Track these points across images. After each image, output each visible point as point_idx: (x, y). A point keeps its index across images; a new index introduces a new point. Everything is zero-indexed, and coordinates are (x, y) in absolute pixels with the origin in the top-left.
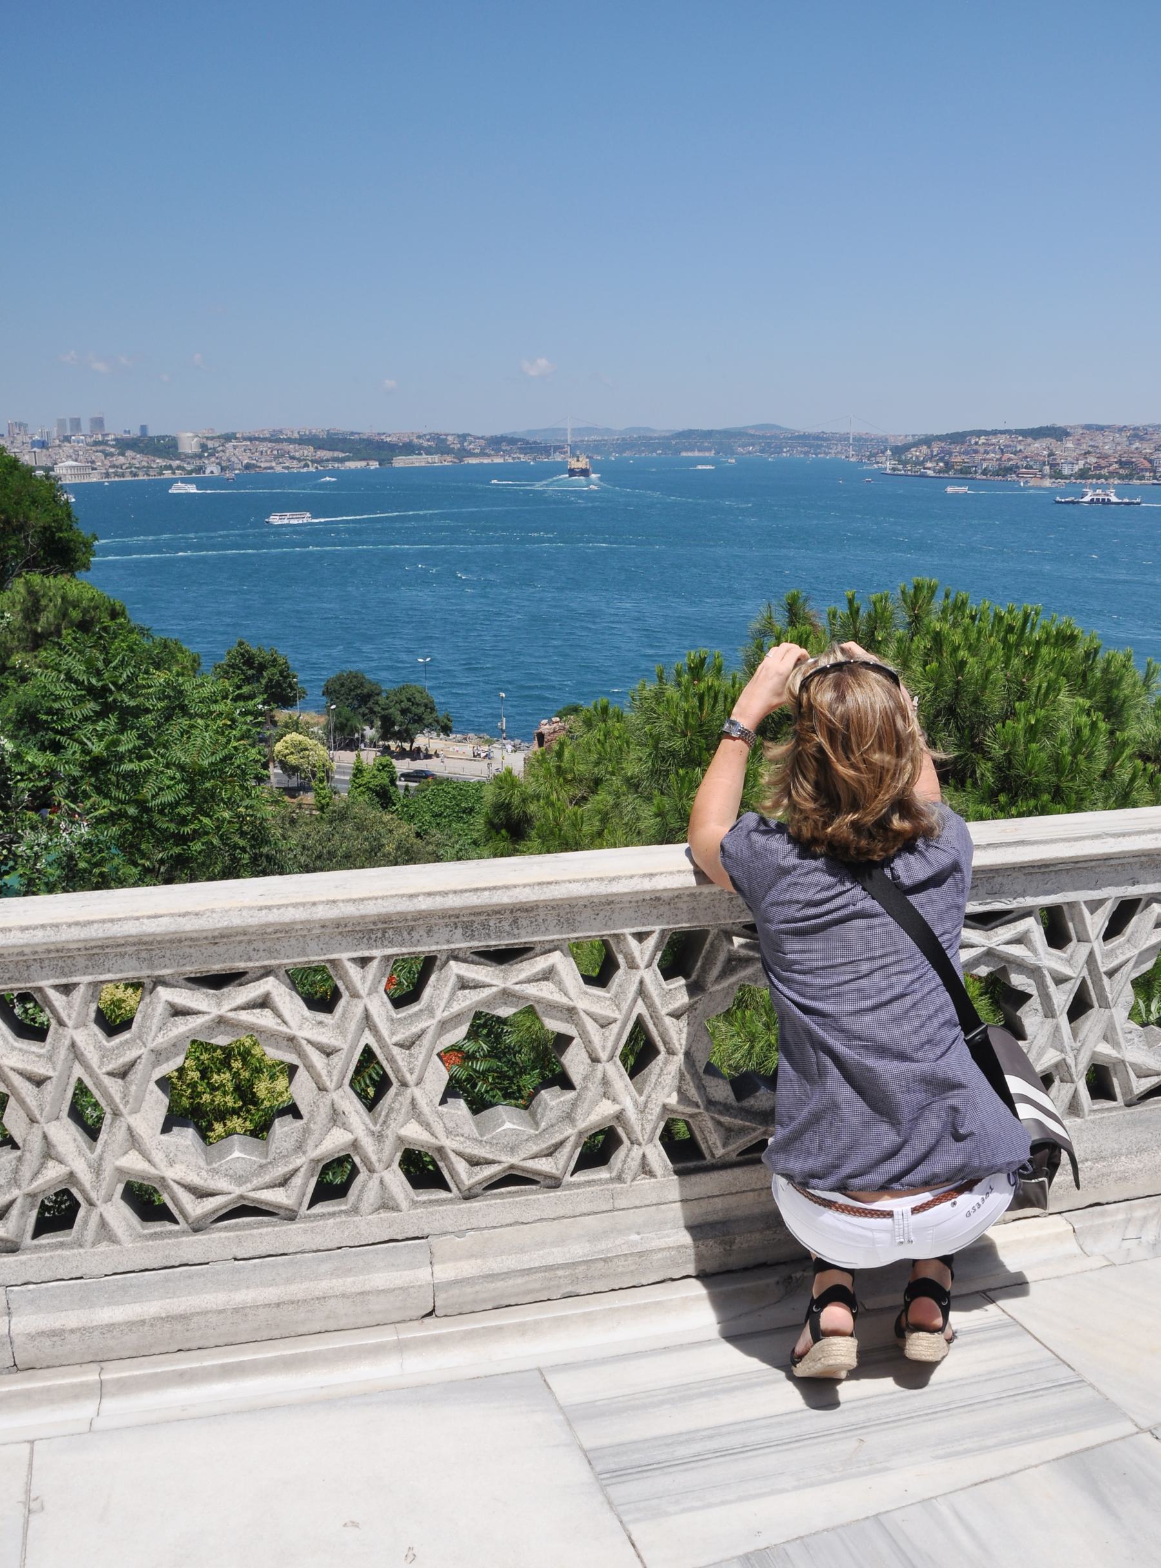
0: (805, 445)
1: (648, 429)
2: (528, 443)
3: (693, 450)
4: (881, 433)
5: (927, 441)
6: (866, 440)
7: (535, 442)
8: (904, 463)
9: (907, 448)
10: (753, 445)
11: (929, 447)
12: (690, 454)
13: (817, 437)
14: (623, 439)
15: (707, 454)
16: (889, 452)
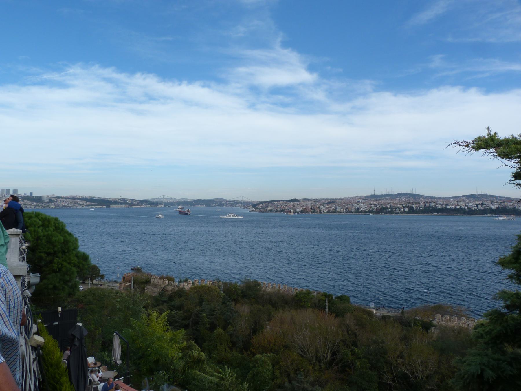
5: (262, 203)
8: (256, 209)
13: (233, 201)
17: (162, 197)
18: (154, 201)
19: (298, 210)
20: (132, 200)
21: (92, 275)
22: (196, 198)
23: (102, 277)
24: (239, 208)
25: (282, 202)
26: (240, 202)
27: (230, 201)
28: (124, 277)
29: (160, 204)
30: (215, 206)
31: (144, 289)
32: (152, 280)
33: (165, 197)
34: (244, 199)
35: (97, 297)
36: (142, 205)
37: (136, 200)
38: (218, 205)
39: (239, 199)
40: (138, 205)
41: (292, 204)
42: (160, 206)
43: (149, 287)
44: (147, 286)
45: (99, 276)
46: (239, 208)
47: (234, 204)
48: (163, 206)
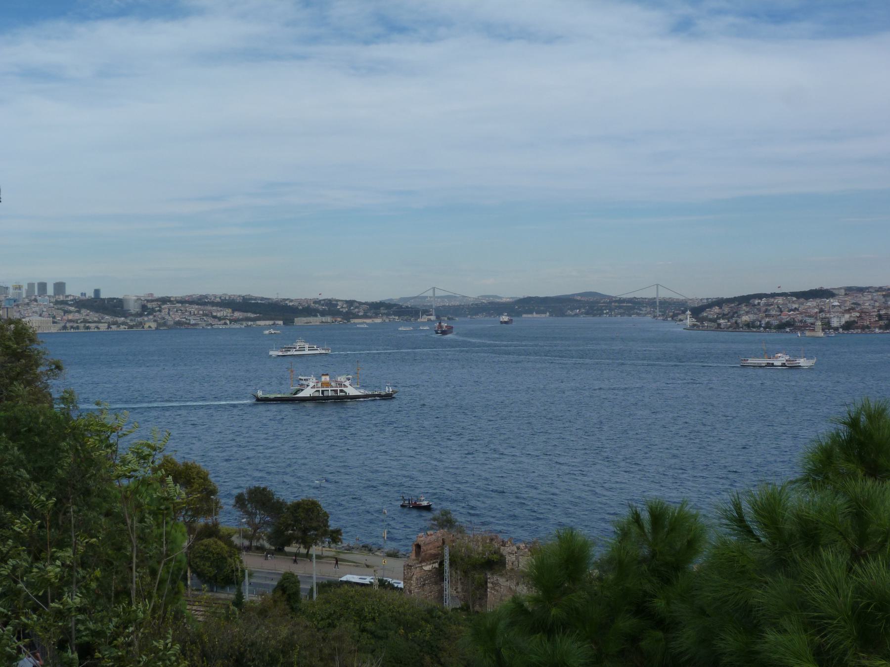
0: (620, 307)
1: (496, 297)
2: (401, 307)
3: (531, 313)
4: (681, 298)
5: (720, 302)
6: (670, 304)
7: (407, 307)
8: (702, 320)
9: (702, 308)
10: (579, 308)
11: (721, 308)
12: (530, 316)
13: (630, 301)
14: (476, 304)
15: (543, 315)
16: (689, 312)
17: (430, 293)
18: (409, 304)
19: (835, 323)
20: (350, 303)
21: (305, 531)
22: (521, 297)
23: (335, 536)
24: (649, 318)
25: (780, 300)
26: (651, 303)
27: (621, 301)
28: (418, 546)
29: (426, 312)
30: (576, 315)
31: (483, 585)
32: (510, 559)
33: (439, 293)
34: (664, 294)
35: (370, 625)
36: (376, 315)
37: (360, 303)
38: (587, 313)
39: (649, 294)
40: (365, 316)
41: (811, 304)
42: (424, 319)
43: (502, 581)
44: (492, 578)
45: (325, 533)
46: (649, 318)
47: (633, 308)
48: (433, 318)
